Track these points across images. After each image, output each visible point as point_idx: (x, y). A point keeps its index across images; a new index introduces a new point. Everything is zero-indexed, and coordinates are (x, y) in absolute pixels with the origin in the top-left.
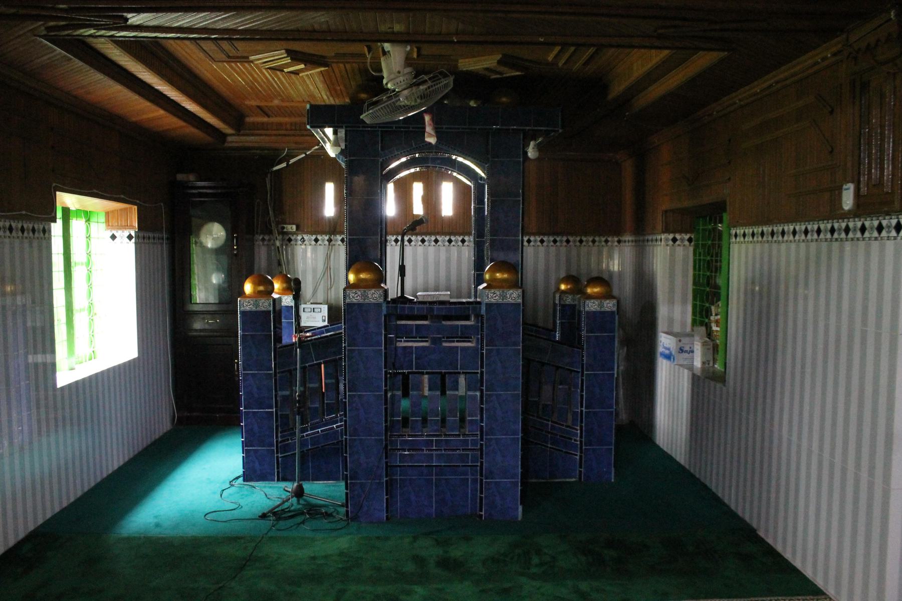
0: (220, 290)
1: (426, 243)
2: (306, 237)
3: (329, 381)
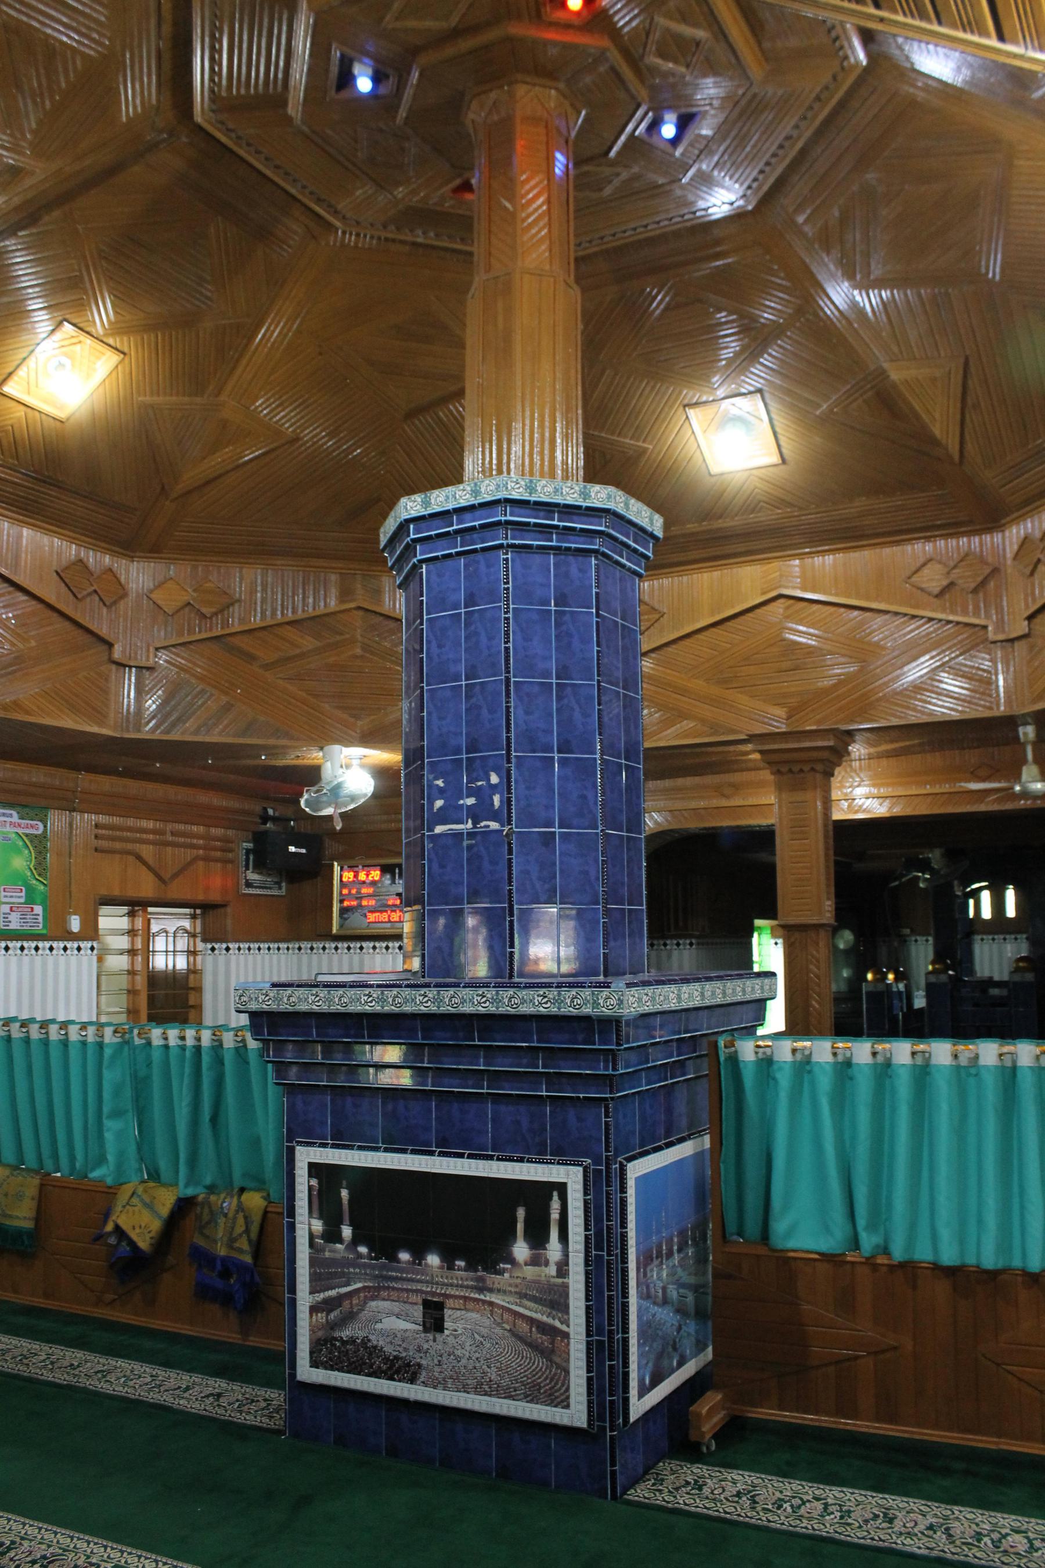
0: (849, 981)
1: (216, 952)
2: (918, 938)
3: (678, 1073)
